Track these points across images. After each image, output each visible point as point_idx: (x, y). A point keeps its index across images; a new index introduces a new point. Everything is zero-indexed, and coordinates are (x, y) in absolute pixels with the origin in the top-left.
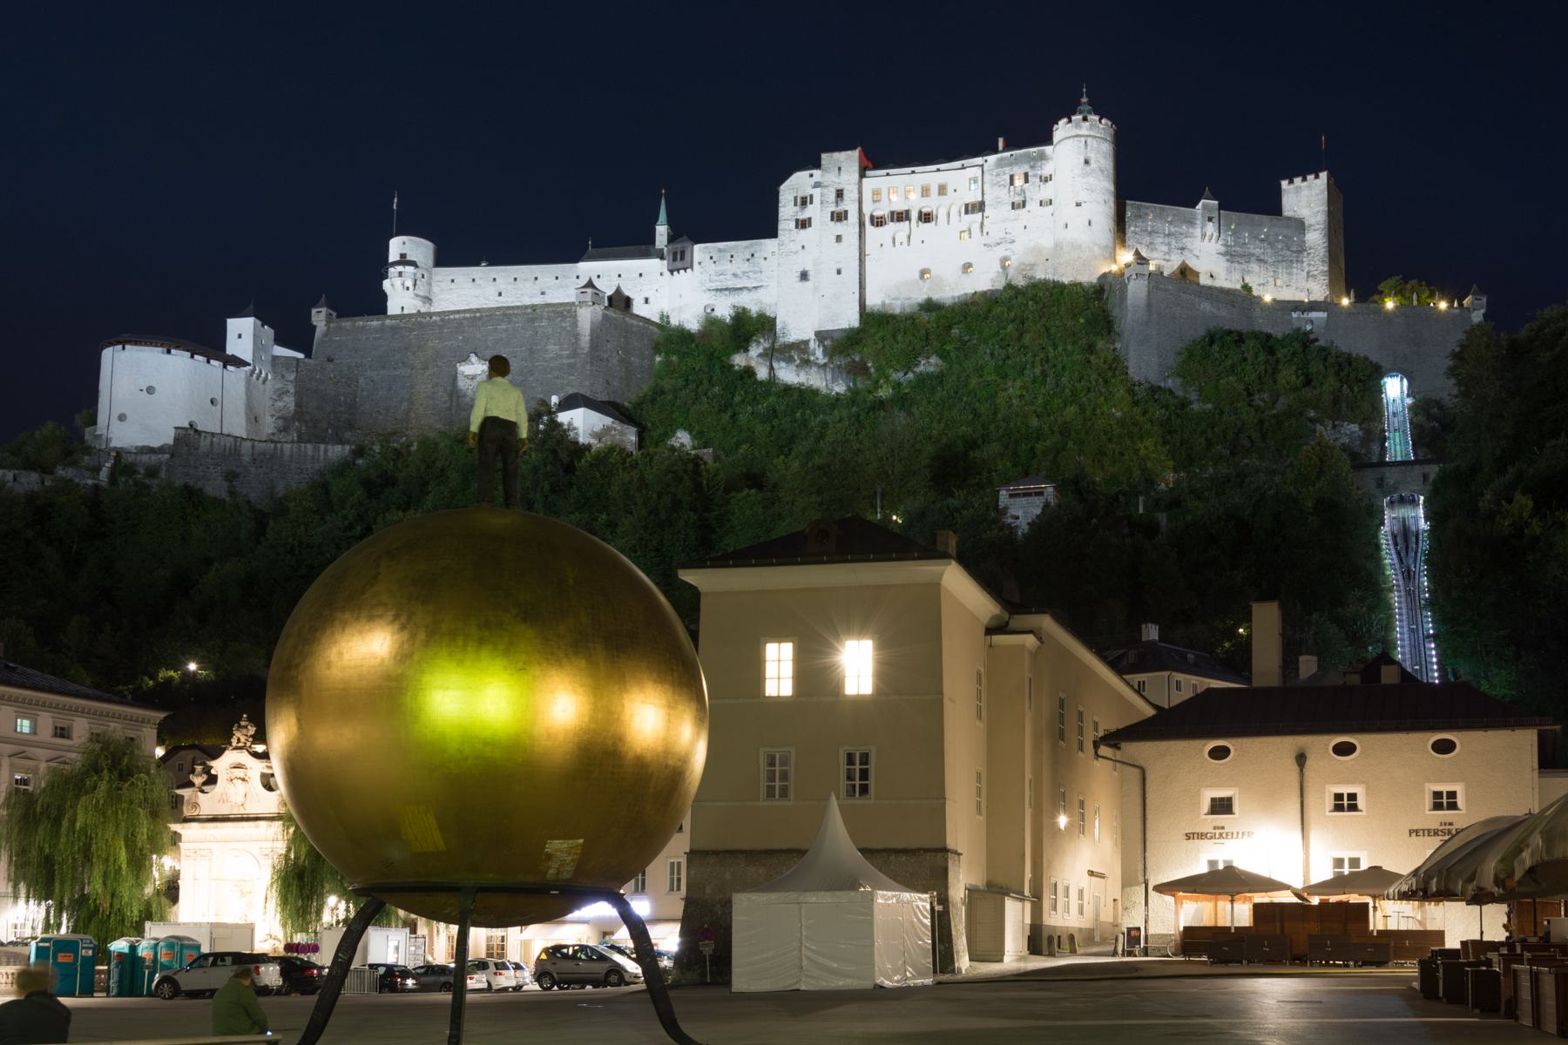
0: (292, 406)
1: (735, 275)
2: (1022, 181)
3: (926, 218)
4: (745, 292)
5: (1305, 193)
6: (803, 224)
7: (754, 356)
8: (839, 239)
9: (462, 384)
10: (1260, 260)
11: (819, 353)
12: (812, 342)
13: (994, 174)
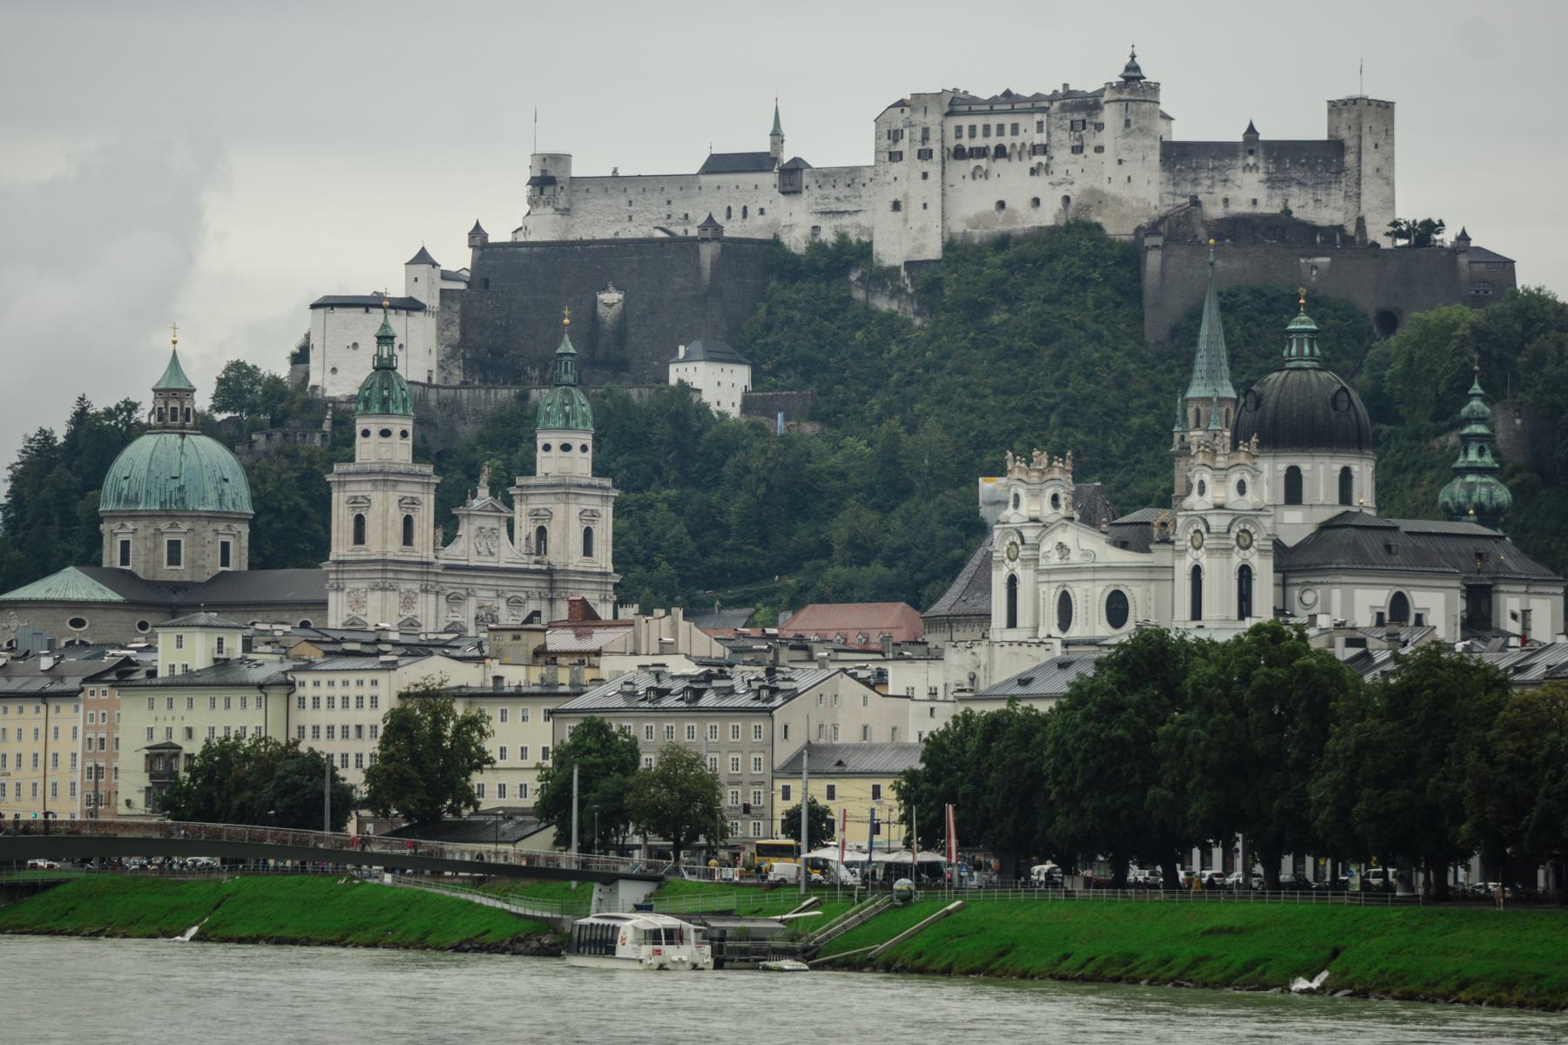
0: (457, 335)
1: (838, 199)
3: (1001, 152)
4: (847, 216)
5: (1345, 115)
6: (895, 157)
8: (925, 176)
9: (601, 310)
10: (1301, 184)
11: (907, 281)
12: (903, 273)
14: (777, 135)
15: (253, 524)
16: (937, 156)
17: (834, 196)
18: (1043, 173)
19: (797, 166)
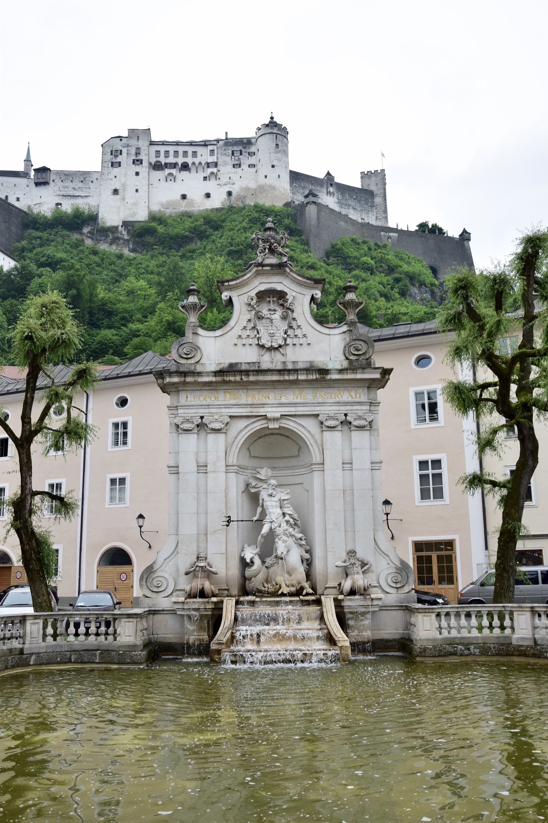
1: (74, 189)
2: (239, 154)
3: (185, 167)
4: (80, 198)
5: (373, 178)
6: (115, 165)
7: (86, 232)
8: (137, 174)
10: (354, 208)
12: (120, 227)
13: (223, 149)
14: (28, 160)
16: (145, 163)
17: (70, 187)
19: (44, 170)
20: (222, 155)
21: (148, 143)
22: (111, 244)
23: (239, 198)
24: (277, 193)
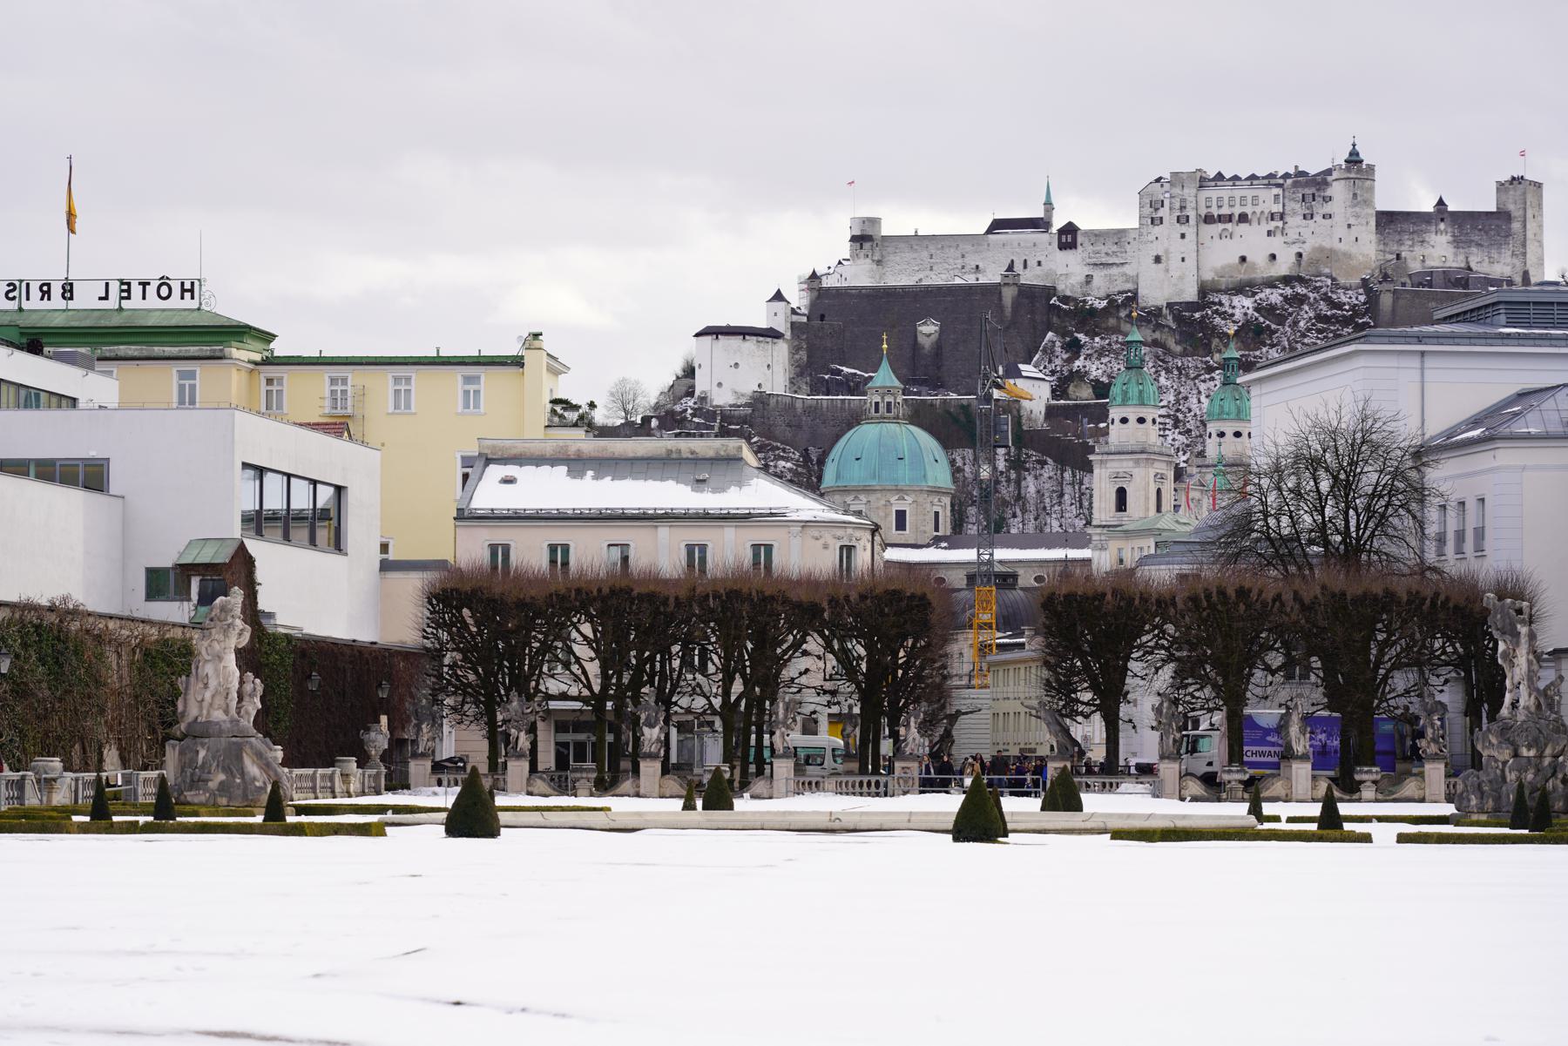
0: (805, 358)
2: (1311, 199)
3: (1243, 218)
4: (1115, 267)
5: (1511, 193)
8: (1183, 236)
9: (921, 339)
10: (1479, 245)
11: (1170, 318)
14: (1049, 205)
15: (953, 497)
16: (1192, 221)
18: (1278, 234)
19: (1070, 230)
20: (1290, 200)
21: (1194, 191)
22: (1154, 331)
23: (1311, 263)
24: (1354, 263)
